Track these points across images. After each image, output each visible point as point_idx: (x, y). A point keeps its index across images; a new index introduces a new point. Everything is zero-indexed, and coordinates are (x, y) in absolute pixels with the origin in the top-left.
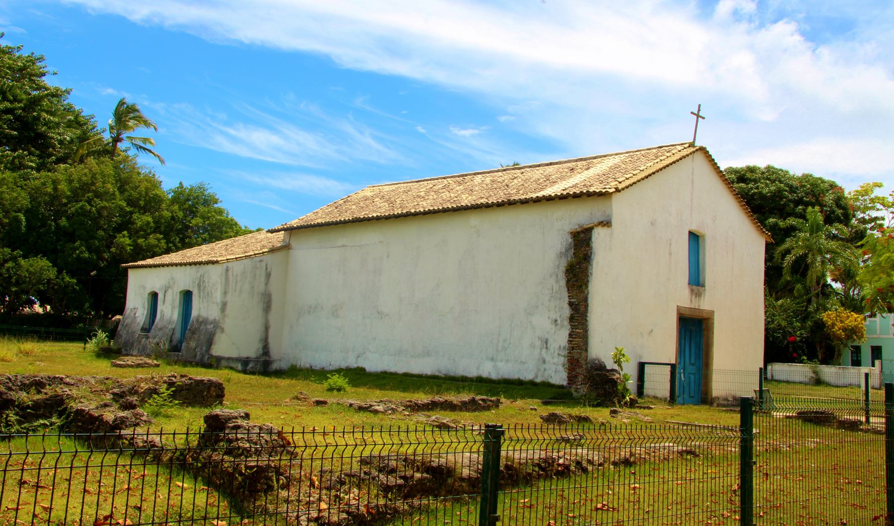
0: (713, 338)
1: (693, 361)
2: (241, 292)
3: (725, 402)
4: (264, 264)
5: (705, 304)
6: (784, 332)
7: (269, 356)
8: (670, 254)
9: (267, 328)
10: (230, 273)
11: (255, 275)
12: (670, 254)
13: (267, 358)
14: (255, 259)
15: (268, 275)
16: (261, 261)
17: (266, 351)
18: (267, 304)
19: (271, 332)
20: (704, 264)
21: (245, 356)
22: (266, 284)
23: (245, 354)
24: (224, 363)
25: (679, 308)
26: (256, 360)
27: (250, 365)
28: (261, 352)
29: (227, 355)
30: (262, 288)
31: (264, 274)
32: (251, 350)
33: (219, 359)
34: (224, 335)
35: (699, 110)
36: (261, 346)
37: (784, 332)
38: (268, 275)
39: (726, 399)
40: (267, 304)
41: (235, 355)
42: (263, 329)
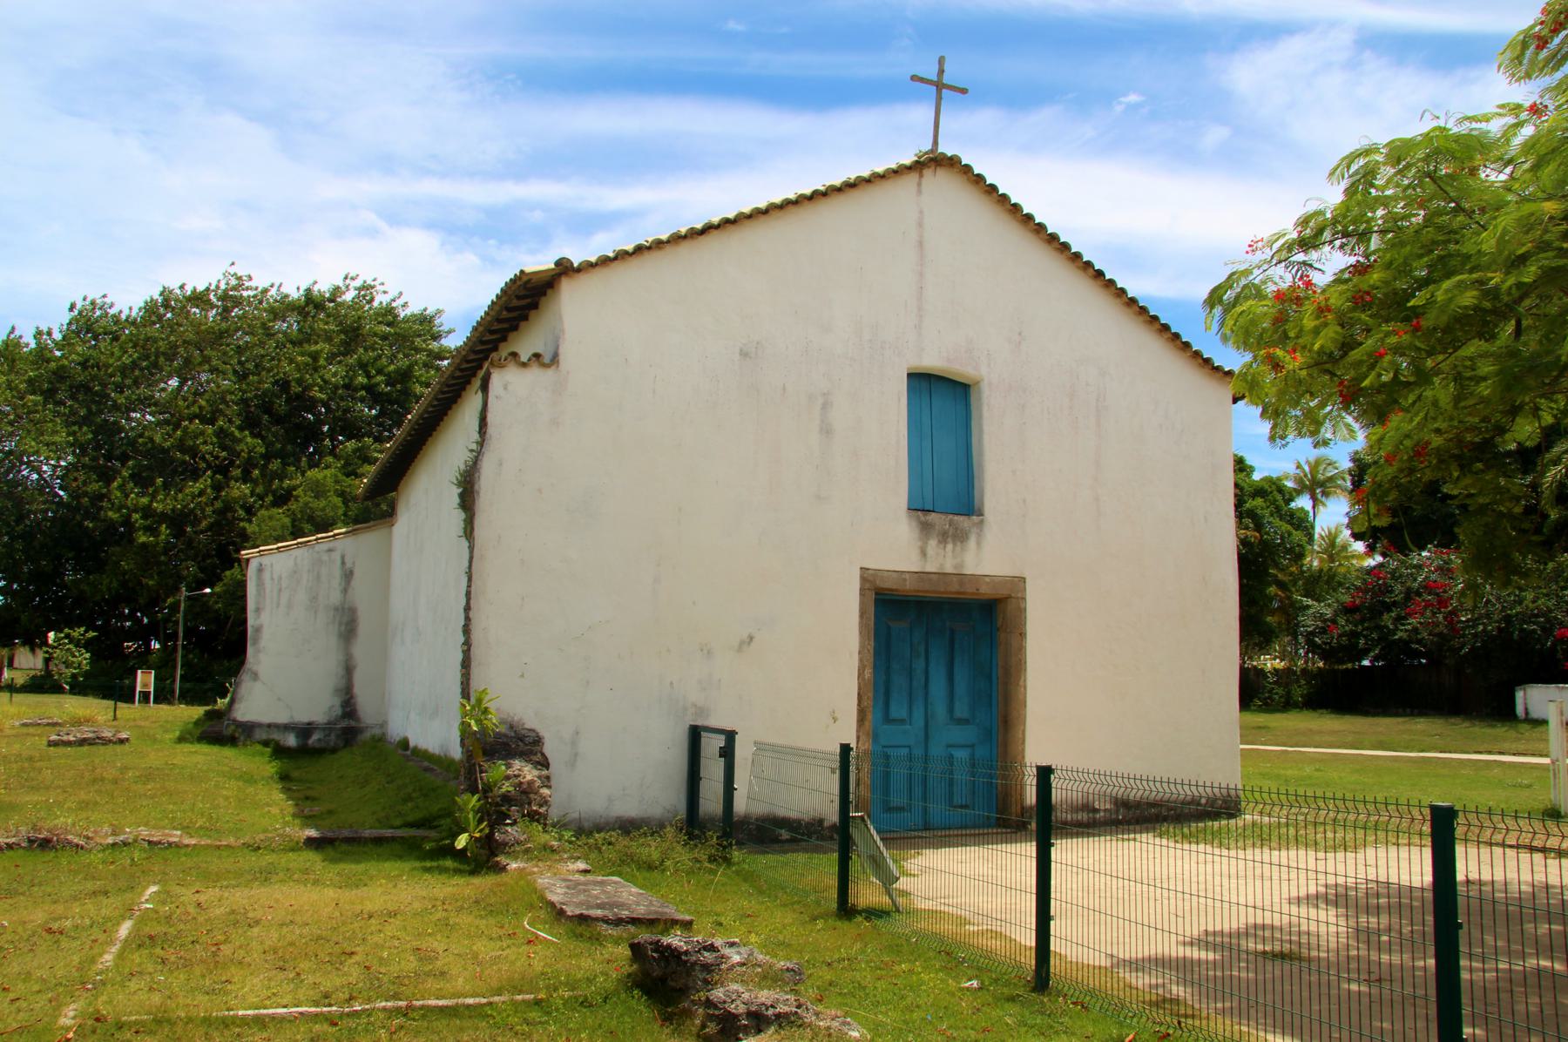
0: (1021, 649)
1: (961, 710)
2: (290, 606)
3: (1083, 816)
4: (337, 556)
5: (984, 559)
6: (1548, 621)
7: (358, 720)
8: (827, 430)
9: (349, 670)
10: (267, 575)
11: (318, 577)
12: (827, 430)
13: (353, 723)
14: (318, 548)
15: (348, 575)
16: (330, 550)
17: (349, 707)
18: (348, 626)
19: (358, 677)
20: (981, 454)
21: (306, 720)
22: (345, 591)
23: (303, 717)
24: (261, 735)
25: (867, 577)
26: (328, 727)
27: (315, 737)
28: (339, 711)
29: (266, 720)
30: (335, 597)
31: (337, 572)
32: (316, 707)
33: (249, 729)
34: (258, 685)
35: (941, 72)
36: (337, 701)
37: (1548, 621)
38: (348, 575)
39: (1087, 807)
40: (348, 626)
41: (282, 718)
42: (341, 672)
